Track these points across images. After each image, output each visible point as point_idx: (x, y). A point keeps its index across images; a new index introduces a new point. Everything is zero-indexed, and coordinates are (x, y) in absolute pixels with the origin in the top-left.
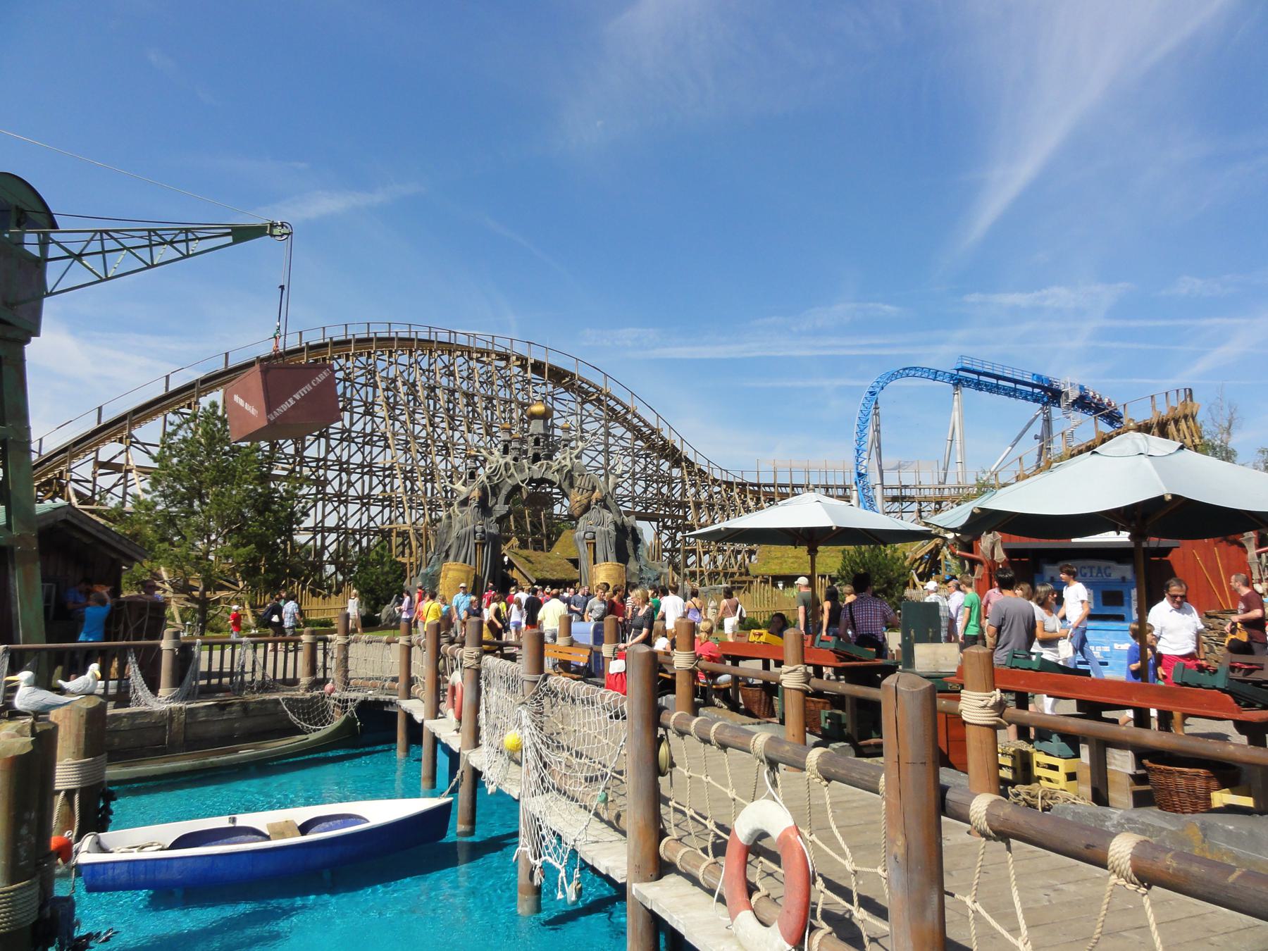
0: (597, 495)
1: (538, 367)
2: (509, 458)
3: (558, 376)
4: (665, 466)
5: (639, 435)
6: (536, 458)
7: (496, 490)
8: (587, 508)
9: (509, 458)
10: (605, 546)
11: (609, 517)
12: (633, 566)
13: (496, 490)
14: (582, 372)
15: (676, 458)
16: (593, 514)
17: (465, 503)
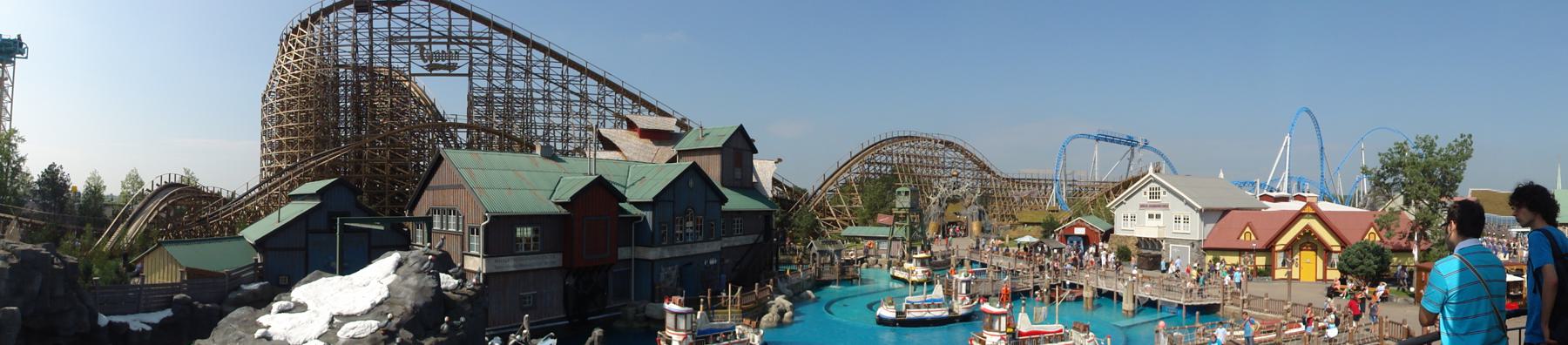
0: (973, 201)
1: (942, 142)
2: (946, 189)
3: (948, 144)
4: (985, 174)
5: (975, 162)
6: (954, 189)
7: (943, 199)
8: (970, 205)
9: (946, 189)
10: (976, 216)
11: (977, 207)
12: (983, 222)
13: (943, 199)
14: (956, 142)
15: (989, 171)
16: (973, 207)
17: (934, 203)
